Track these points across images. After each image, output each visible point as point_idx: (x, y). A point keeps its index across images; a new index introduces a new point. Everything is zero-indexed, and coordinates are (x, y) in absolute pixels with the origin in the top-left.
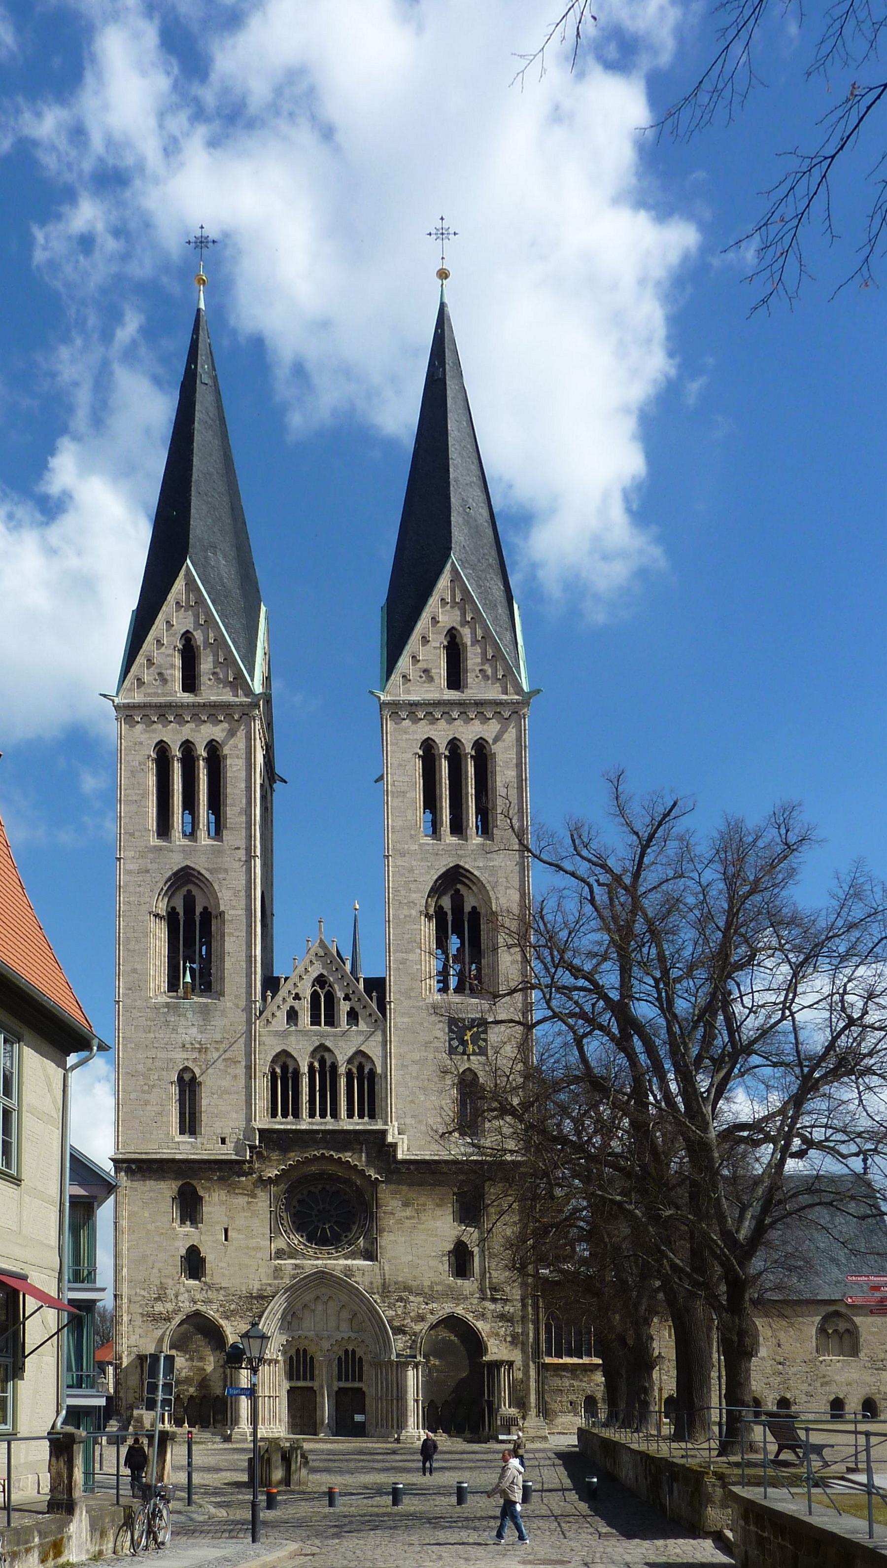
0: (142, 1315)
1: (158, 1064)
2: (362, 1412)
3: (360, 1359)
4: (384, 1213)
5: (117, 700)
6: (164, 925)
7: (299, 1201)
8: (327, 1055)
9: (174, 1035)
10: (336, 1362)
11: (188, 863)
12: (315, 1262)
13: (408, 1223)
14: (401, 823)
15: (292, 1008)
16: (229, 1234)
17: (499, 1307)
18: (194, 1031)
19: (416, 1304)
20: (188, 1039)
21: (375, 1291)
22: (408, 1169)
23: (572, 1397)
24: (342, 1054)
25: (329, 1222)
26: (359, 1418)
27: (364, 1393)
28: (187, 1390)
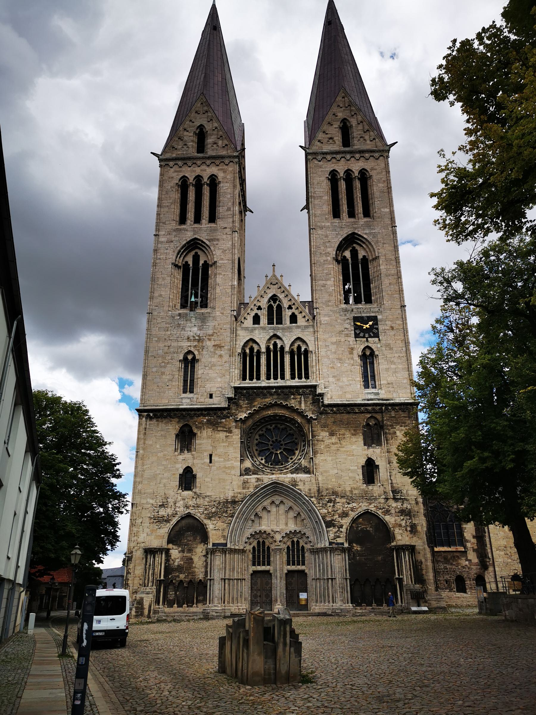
0: (150, 518)
1: (172, 350)
2: (305, 591)
3: (303, 547)
4: (317, 440)
5: (161, 157)
6: (181, 272)
7: (260, 435)
8: (278, 341)
9: (182, 332)
10: (286, 550)
11: (196, 236)
12: (271, 476)
13: (334, 447)
14: (319, 212)
15: (256, 314)
16: (213, 458)
17: (399, 504)
18: (195, 329)
19: (341, 504)
20: (192, 334)
21: (313, 495)
22: (332, 410)
23: (447, 577)
24: (287, 341)
25: (280, 449)
26: (303, 596)
27: (306, 574)
28: (178, 576)
